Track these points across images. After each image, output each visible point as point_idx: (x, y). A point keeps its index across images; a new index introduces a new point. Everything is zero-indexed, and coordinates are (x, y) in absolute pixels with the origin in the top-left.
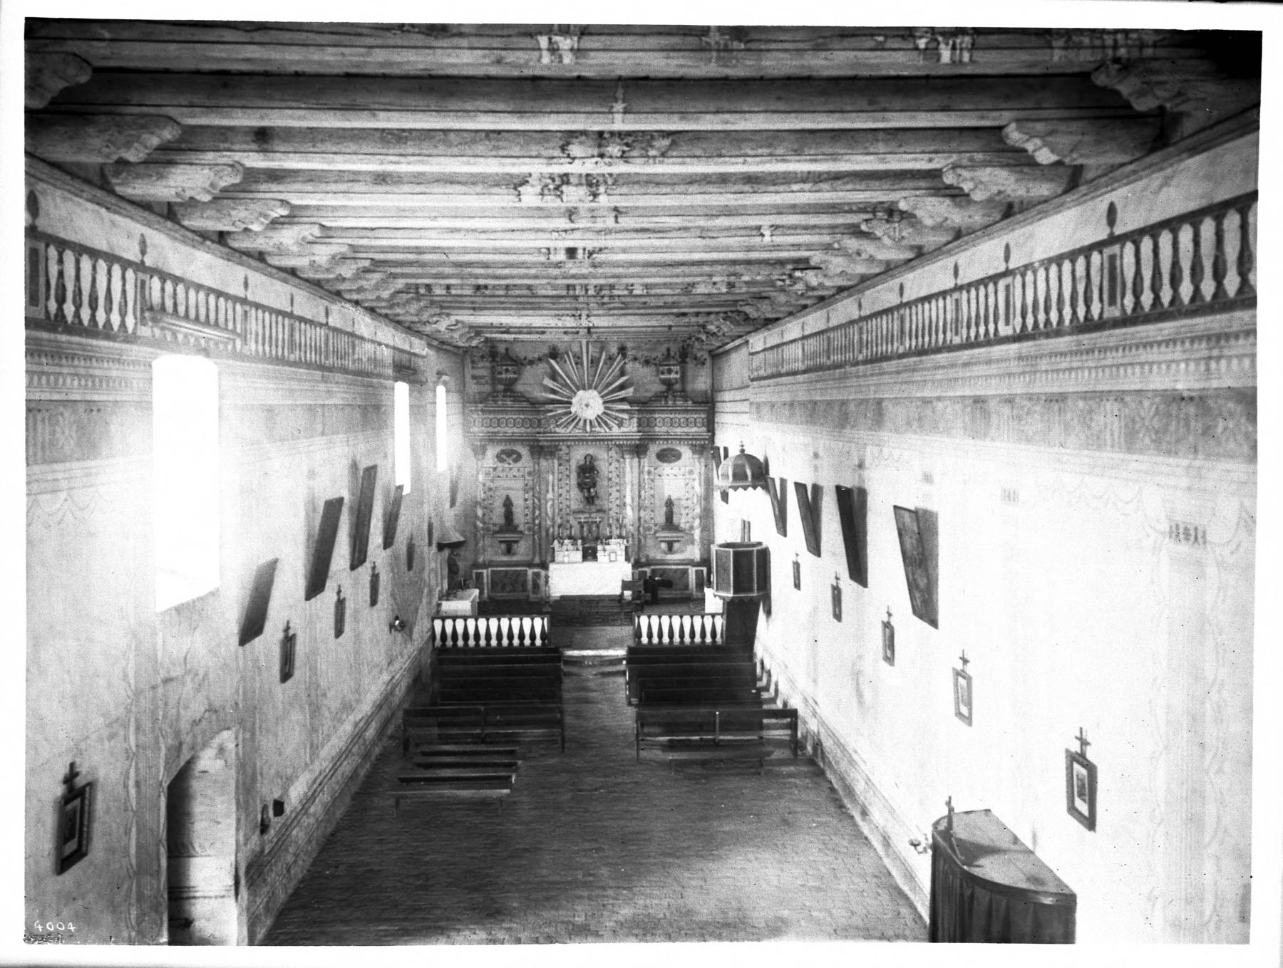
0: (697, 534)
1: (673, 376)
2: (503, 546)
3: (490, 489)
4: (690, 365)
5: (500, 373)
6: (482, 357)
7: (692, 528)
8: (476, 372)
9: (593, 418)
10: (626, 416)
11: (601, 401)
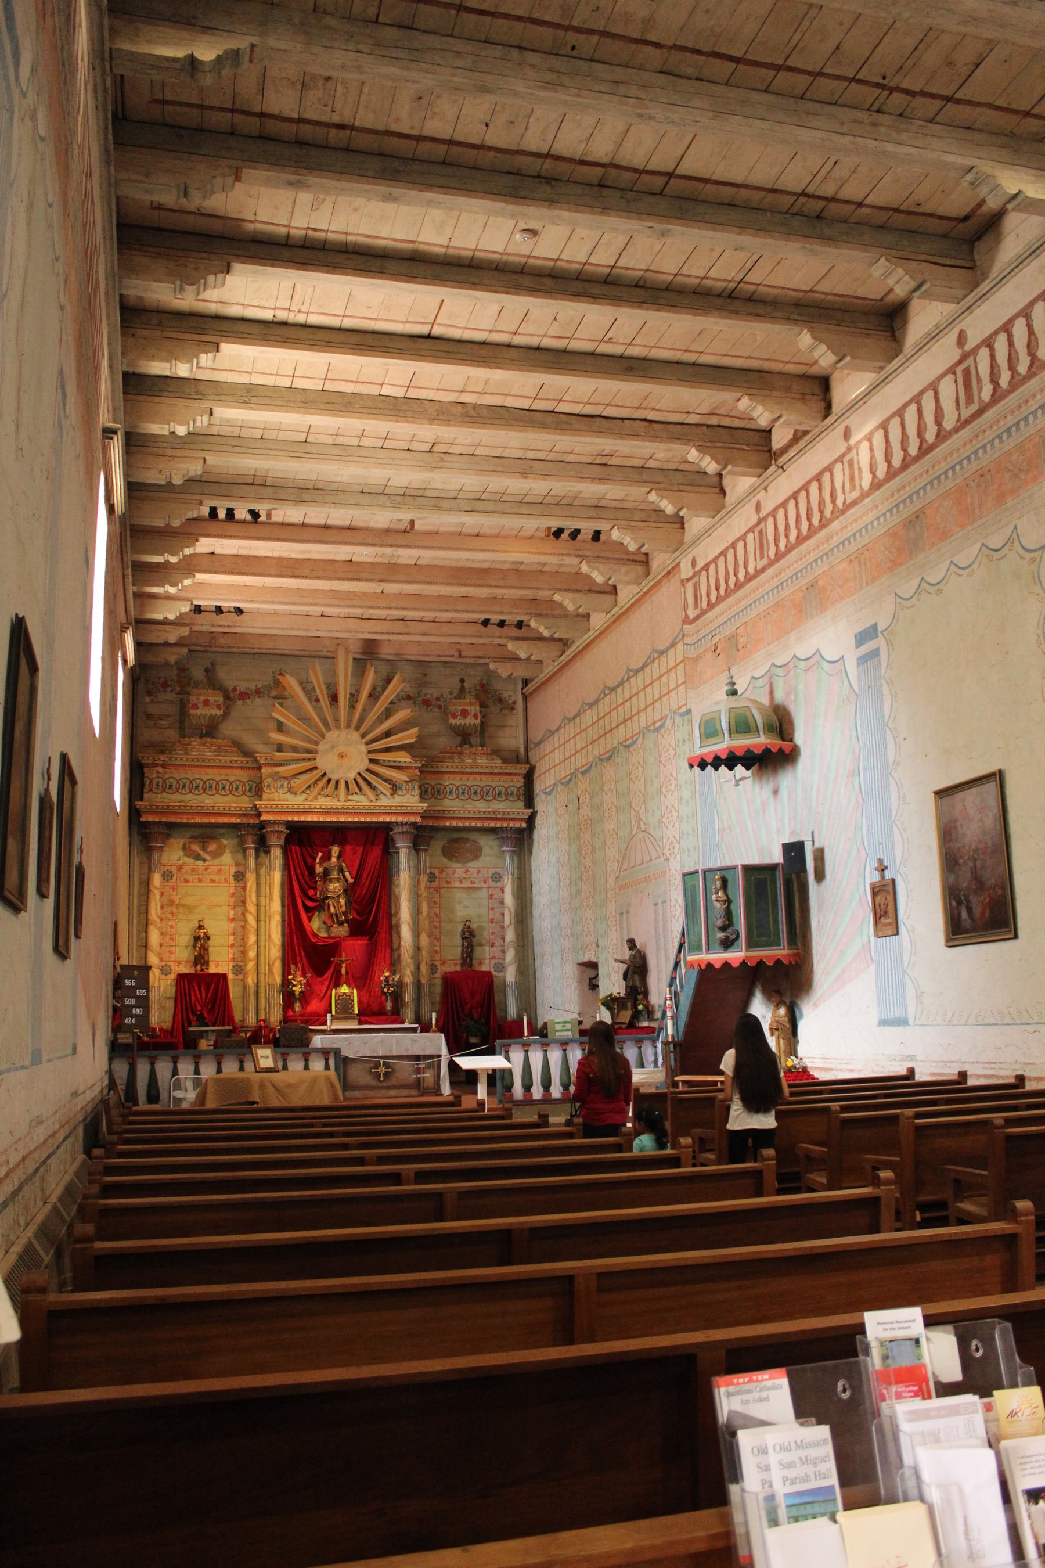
0: (510, 976)
1: (469, 721)
3: (172, 902)
4: (494, 709)
5: (195, 707)
6: (165, 685)
8: (153, 709)
9: (352, 775)
10: (400, 776)
11: (364, 749)
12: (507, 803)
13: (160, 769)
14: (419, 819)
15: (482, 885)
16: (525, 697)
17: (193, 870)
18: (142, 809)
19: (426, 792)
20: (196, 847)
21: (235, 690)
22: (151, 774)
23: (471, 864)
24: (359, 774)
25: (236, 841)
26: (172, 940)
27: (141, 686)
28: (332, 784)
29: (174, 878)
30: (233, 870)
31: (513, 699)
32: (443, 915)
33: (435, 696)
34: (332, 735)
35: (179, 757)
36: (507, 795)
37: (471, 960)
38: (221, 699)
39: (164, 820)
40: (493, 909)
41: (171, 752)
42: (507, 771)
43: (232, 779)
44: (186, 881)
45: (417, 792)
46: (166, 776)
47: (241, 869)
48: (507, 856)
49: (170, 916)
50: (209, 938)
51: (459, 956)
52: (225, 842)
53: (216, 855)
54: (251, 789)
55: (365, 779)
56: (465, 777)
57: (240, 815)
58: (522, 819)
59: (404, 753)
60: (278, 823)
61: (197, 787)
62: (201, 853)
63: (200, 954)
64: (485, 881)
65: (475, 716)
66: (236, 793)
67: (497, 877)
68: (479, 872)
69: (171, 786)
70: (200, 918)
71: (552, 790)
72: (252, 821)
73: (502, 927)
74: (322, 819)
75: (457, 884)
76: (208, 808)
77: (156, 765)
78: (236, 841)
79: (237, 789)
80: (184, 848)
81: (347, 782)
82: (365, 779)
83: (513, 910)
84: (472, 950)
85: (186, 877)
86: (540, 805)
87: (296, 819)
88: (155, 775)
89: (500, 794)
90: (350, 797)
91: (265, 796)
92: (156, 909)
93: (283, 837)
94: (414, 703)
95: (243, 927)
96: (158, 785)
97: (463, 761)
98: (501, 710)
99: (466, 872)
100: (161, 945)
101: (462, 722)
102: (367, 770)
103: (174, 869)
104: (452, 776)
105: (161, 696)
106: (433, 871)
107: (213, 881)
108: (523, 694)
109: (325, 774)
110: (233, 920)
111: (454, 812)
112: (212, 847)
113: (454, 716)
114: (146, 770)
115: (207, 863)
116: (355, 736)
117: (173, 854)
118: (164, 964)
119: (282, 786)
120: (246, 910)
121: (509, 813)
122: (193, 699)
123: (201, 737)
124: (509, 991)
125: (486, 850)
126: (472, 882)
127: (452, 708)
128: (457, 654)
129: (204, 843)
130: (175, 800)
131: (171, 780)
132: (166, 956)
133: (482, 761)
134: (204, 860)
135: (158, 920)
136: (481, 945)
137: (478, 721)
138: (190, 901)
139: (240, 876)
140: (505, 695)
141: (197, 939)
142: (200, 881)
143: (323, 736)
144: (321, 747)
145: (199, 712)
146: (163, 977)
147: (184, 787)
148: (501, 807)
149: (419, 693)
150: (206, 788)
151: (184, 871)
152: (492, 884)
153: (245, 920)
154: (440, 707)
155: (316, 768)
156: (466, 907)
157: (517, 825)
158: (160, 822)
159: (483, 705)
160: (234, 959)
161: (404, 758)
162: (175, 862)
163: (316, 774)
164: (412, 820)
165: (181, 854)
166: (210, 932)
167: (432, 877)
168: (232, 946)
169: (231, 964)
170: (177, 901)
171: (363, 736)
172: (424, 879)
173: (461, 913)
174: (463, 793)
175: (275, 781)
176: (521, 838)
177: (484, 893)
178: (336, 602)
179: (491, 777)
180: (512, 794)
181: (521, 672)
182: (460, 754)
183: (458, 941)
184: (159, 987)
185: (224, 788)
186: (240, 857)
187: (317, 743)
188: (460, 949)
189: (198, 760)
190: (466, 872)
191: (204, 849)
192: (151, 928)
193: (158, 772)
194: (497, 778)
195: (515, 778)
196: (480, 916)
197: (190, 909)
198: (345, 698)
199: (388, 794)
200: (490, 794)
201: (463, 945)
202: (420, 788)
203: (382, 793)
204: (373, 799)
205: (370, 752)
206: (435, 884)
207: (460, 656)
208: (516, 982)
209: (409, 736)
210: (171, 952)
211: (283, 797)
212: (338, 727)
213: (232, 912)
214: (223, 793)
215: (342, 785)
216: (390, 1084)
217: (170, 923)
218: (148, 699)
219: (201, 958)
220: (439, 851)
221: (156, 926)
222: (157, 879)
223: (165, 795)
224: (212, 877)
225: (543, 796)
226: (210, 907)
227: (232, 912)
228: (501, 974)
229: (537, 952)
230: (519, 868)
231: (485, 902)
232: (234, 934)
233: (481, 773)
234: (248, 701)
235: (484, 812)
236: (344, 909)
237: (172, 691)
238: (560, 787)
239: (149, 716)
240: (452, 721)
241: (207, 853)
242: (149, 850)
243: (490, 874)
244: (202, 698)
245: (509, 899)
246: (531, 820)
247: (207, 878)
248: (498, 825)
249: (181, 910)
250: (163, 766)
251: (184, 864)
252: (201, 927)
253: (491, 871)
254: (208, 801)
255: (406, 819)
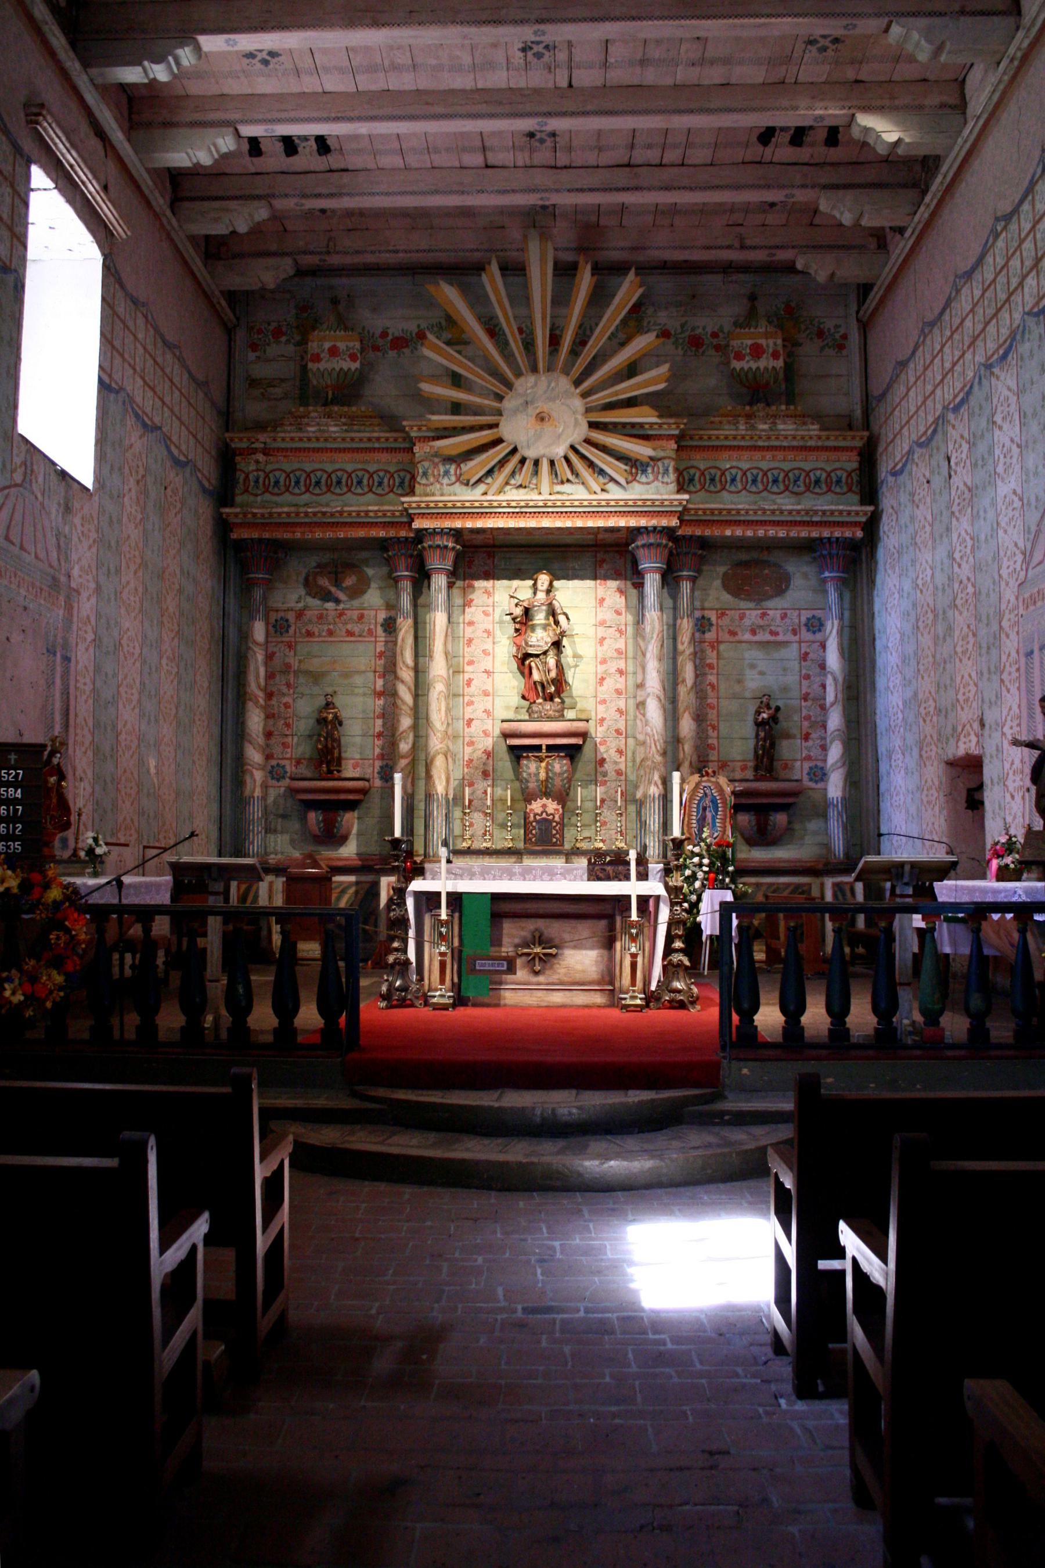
0: (835, 788)
1: (764, 363)
2: (314, 817)
3: (287, 668)
4: (809, 349)
5: (317, 358)
6: (278, 333)
7: (820, 775)
8: (261, 371)
9: (560, 450)
11: (578, 404)
12: (829, 496)
13: (260, 457)
14: (674, 522)
15: (790, 637)
16: (865, 326)
17: (320, 617)
18: (233, 520)
19: (691, 480)
20: (324, 582)
21: (384, 334)
22: (247, 466)
23: (770, 604)
24: (573, 448)
25: (385, 570)
26: (288, 725)
27: (241, 335)
28: (528, 465)
29: (291, 631)
30: (382, 615)
31: (842, 331)
32: (722, 687)
33: (709, 330)
34: (526, 384)
35: (286, 436)
36: (829, 484)
37: (772, 759)
38: (358, 345)
39: (266, 535)
40: (807, 677)
41: (274, 430)
42: (830, 444)
43: (372, 468)
44: (310, 634)
45: (672, 476)
46: (269, 468)
47: (392, 613)
48: (831, 588)
49: (285, 689)
50: (341, 724)
51: (751, 756)
52: (370, 572)
53: (357, 592)
54: (402, 483)
55: (583, 457)
56: (758, 455)
57: (385, 525)
58: (856, 524)
59: (646, 409)
60: (442, 532)
61: (318, 483)
62: (333, 589)
63: (326, 746)
64: (794, 632)
65: (775, 355)
66: (380, 491)
67: (815, 625)
68: (784, 617)
69: (277, 482)
70: (329, 690)
71: (904, 465)
72: (403, 534)
73: (823, 707)
74: (512, 523)
75: (747, 636)
76: (332, 515)
77: (254, 451)
78: (385, 570)
79: (380, 484)
80: (307, 583)
81: (552, 463)
82: (583, 457)
83: (840, 679)
84: (773, 745)
85: (310, 627)
86: (887, 501)
87: (469, 524)
88: (253, 467)
89: (817, 482)
90: (558, 488)
91: (418, 489)
92: (257, 677)
93: (451, 555)
94: (676, 343)
95: (394, 704)
96: (257, 481)
97: (753, 427)
98: (822, 349)
99: (763, 615)
100: (268, 735)
101: (753, 365)
102: (588, 441)
103: (291, 616)
104: (735, 454)
105: (273, 350)
106: (707, 614)
107: (350, 633)
108: (858, 320)
109: (515, 450)
110: (379, 694)
111: (738, 511)
112: (350, 581)
113: (739, 356)
114: (238, 459)
115: (342, 606)
116: (564, 383)
117: (291, 596)
118: (274, 762)
119: (447, 473)
120: (397, 678)
121: (832, 512)
122: (313, 346)
123: (325, 405)
124: (833, 813)
125: (797, 581)
126: (772, 633)
127: (735, 343)
128: (737, 245)
129: (336, 573)
130: (284, 505)
131: (277, 473)
132: (277, 750)
133: (786, 427)
134: (337, 601)
135: (261, 694)
136: (788, 736)
137: (780, 364)
138: (315, 665)
139: (390, 626)
140: (829, 324)
141: (322, 721)
142: (330, 633)
143: (509, 386)
144: (508, 404)
145: (322, 366)
146: (274, 782)
147: (297, 483)
148: (823, 504)
149: (682, 326)
150: (332, 484)
151: (305, 619)
152: (806, 635)
153: (395, 694)
154: (717, 348)
155: (499, 441)
156: (762, 673)
157: (848, 534)
158: (260, 540)
159: (791, 344)
160: (382, 757)
161: (645, 416)
162: (292, 604)
163: (501, 451)
164: (664, 522)
165: (302, 591)
166: (344, 714)
167: (702, 625)
168: (379, 735)
169: (378, 764)
170: (295, 666)
171: (577, 383)
172: (686, 626)
173: (753, 683)
174: (754, 481)
175: (436, 465)
176: (854, 558)
177: (792, 652)
178: (483, 108)
179: (803, 455)
180: (839, 482)
181: (852, 269)
182: (749, 416)
183: (748, 729)
184: (264, 798)
185: (360, 483)
186: (391, 594)
187: (500, 398)
188: (752, 743)
189: (318, 439)
190: (763, 615)
191: (337, 583)
192: (250, 705)
193: (257, 462)
194: (813, 456)
195: (844, 456)
196: (785, 689)
197: (316, 677)
198: (544, 319)
199: (622, 481)
200: (800, 483)
201: (757, 735)
202: (680, 472)
203: (612, 479)
204: (598, 489)
205: (588, 410)
206: (710, 636)
207: (743, 247)
208: (844, 798)
209: (653, 379)
210: (285, 745)
211: (447, 489)
212: (534, 369)
213: (380, 683)
214: (359, 491)
215: (545, 466)
216: (555, 978)
217: (285, 700)
218: (252, 356)
219: (327, 754)
220: (718, 583)
221: (256, 703)
222: (259, 631)
223: (267, 497)
224: (349, 627)
225: (891, 479)
226: (347, 675)
227: (380, 683)
228: (820, 785)
229: (882, 749)
230: (853, 610)
231: (795, 665)
232: (383, 716)
233: (784, 448)
234: (405, 350)
235: (790, 512)
236: (553, 674)
237: (288, 342)
238: (918, 451)
239: (253, 382)
240: (737, 365)
241: (342, 589)
242: (246, 587)
243: (803, 619)
244: (327, 345)
245: (833, 659)
246: (872, 526)
247: (341, 629)
248: (815, 534)
249: (302, 680)
250: (266, 452)
251: (306, 608)
252: (328, 705)
253: (805, 615)
254: (336, 504)
255: (653, 522)
